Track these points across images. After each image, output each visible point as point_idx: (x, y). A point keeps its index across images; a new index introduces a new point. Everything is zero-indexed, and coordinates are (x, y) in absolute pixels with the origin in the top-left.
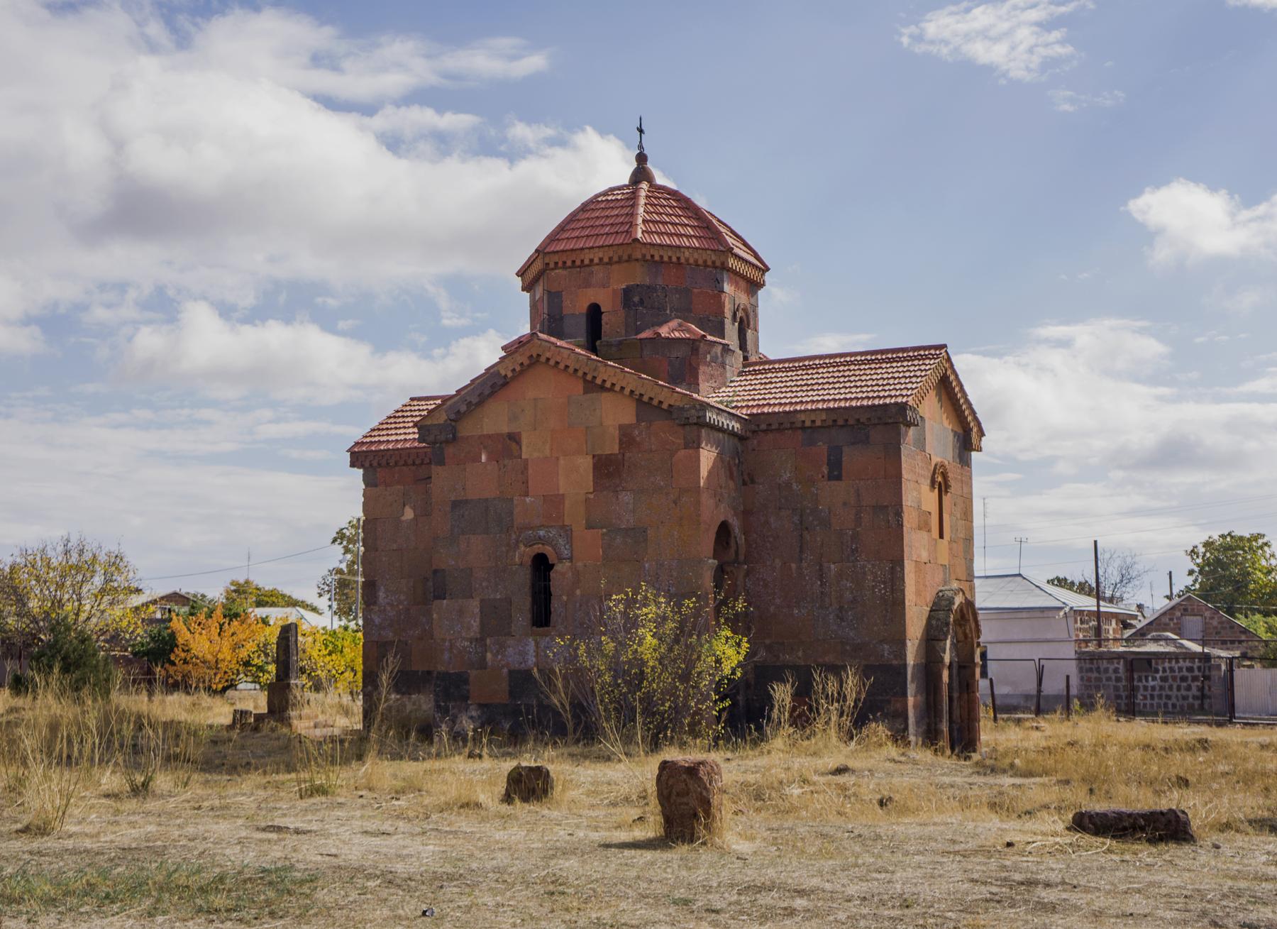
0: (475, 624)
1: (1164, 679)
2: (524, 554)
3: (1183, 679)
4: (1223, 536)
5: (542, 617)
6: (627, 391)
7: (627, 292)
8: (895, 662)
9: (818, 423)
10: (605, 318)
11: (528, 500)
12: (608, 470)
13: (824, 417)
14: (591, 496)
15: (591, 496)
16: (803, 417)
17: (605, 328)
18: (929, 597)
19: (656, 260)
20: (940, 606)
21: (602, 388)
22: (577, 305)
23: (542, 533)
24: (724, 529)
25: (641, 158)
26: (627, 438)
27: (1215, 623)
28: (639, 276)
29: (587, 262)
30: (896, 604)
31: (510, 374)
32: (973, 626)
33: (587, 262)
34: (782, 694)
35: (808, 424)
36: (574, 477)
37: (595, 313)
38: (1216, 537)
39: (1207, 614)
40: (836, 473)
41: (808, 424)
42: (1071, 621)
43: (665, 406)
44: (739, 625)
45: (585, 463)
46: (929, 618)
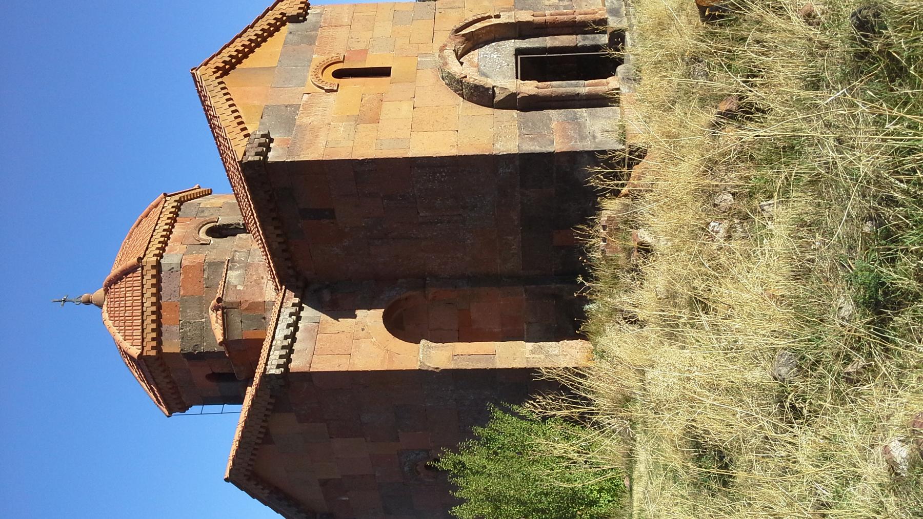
6: (265, 424)
8: (517, 163)
9: (279, 232)
10: (217, 371)
11: (377, 475)
13: (271, 228)
14: (369, 439)
15: (369, 439)
16: (275, 245)
17: (225, 371)
21: (267, 434)
23: (406, 469)
29: (169, 386)
31: (267, 491)
32: (478, 26)
33: (169, 386)
35: (280, 239)
41: (280, 239)
43: (273, 401)
46: (470, 100)
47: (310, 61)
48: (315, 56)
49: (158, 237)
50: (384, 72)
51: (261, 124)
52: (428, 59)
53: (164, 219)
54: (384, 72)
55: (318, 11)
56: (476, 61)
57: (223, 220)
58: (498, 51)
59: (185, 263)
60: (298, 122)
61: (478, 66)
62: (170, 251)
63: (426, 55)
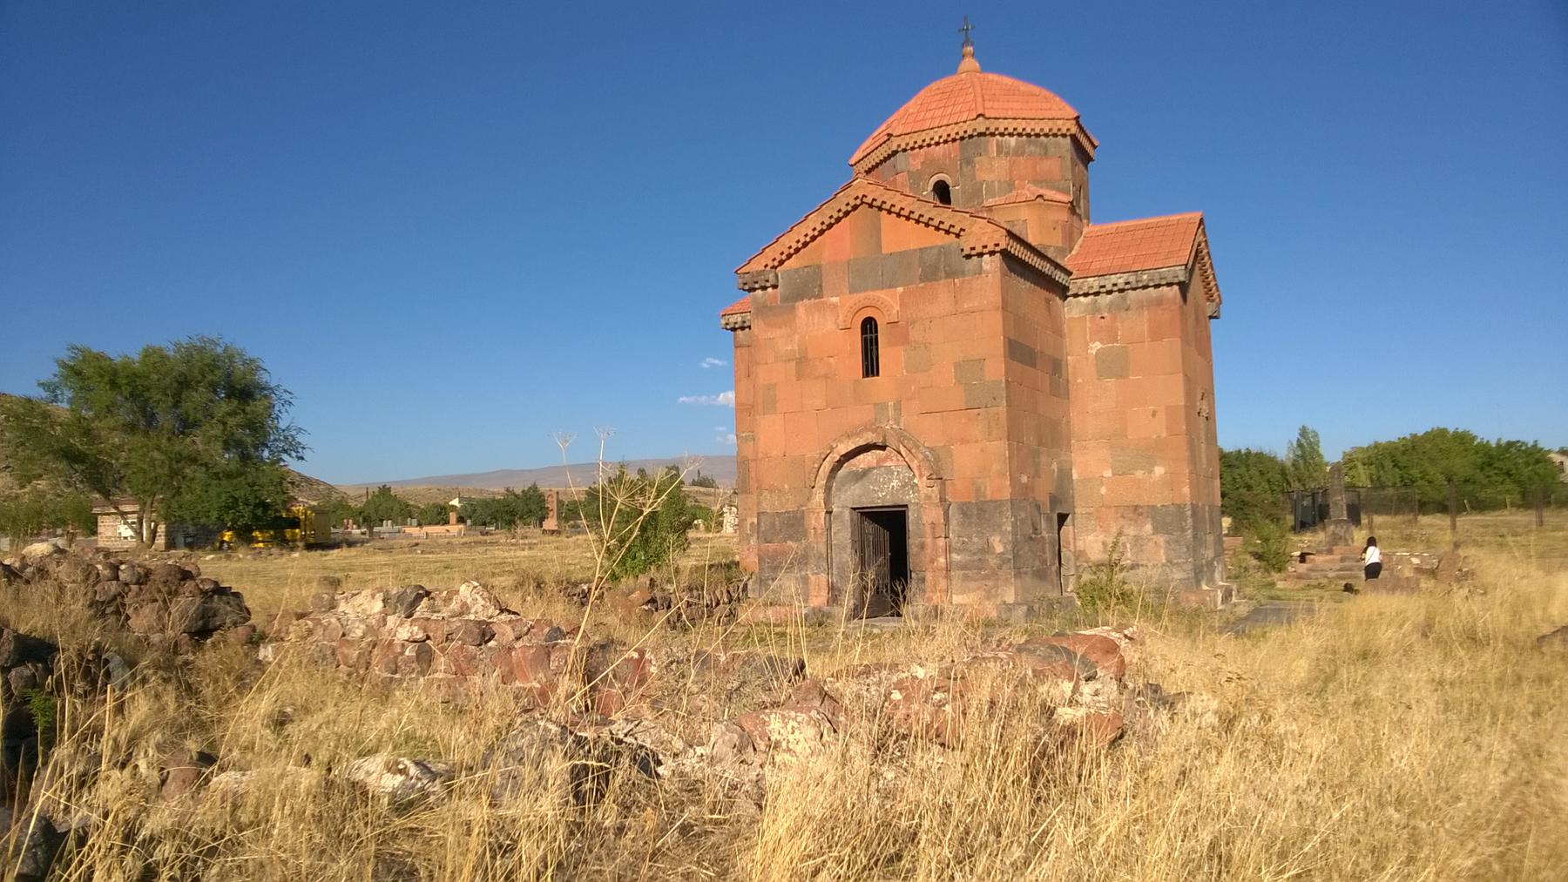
47: (891, 286)
48: (900, 289)
49: (919, 138)
50: (871, 366)
51: (797, 271)
52: (891, 412)
53: (944, 132)
54: (871, 366)
55: (986, 267)
56: (888, 464)
57: (955, 191)
58: (903, 486)
59: (899, 177)
60: (799, 304)
61: (879, 467)
62: (914, 157)
63: (898, 407)
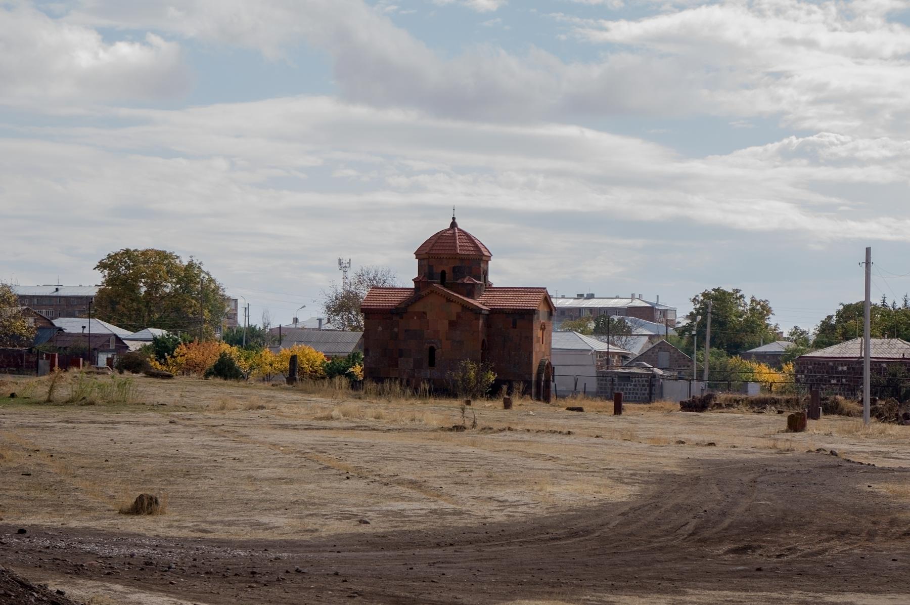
0: (412, 365)
1: (635, 385)
2: (427, 346)
3: (644, 385)
4: (714, 290)
5: (432, 363)
7: (454, 268)
12: (452, 324)
18: (539, 361)
19: (463, 259)
20: (541, 364)
22: (438, 269)
24: (484, 341)
25: (454, 219)
26: (459, 316)
27: (675, 355)
28: (458, 264)
30: (530, 363)
34: (505, 388)
36: (443, 326)
37: (443, 273)
38: (710, 290)
39: (672, 351)
40: (514, 326)
42: (595, 356)
44: (493, 369)
45: (446, 322)
